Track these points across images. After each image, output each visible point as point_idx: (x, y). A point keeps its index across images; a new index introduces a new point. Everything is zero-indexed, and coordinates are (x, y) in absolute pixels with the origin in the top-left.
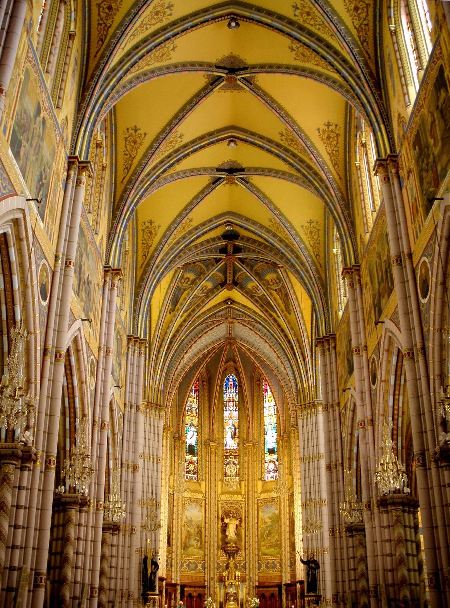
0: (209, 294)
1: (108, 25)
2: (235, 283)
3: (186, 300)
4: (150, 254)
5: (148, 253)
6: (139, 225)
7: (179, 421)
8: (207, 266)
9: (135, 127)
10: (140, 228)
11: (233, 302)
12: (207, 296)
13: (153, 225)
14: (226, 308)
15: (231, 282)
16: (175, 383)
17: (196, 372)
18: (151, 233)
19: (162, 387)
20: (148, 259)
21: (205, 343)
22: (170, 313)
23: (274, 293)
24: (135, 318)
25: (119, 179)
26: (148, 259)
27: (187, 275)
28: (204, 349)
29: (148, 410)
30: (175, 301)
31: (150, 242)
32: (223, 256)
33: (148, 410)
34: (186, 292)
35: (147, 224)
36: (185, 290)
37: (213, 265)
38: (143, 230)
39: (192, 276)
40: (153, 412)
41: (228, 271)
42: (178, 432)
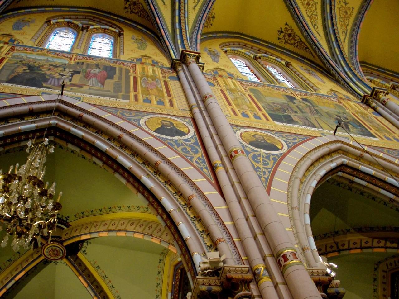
5: (305, 45)
6: (279, 44)
9: (279, 31)
10: (283, 45)
13: (283, 30)
20: (310, 48)
25: (311, 58)
31: (298, 38)
38: (286, 42)
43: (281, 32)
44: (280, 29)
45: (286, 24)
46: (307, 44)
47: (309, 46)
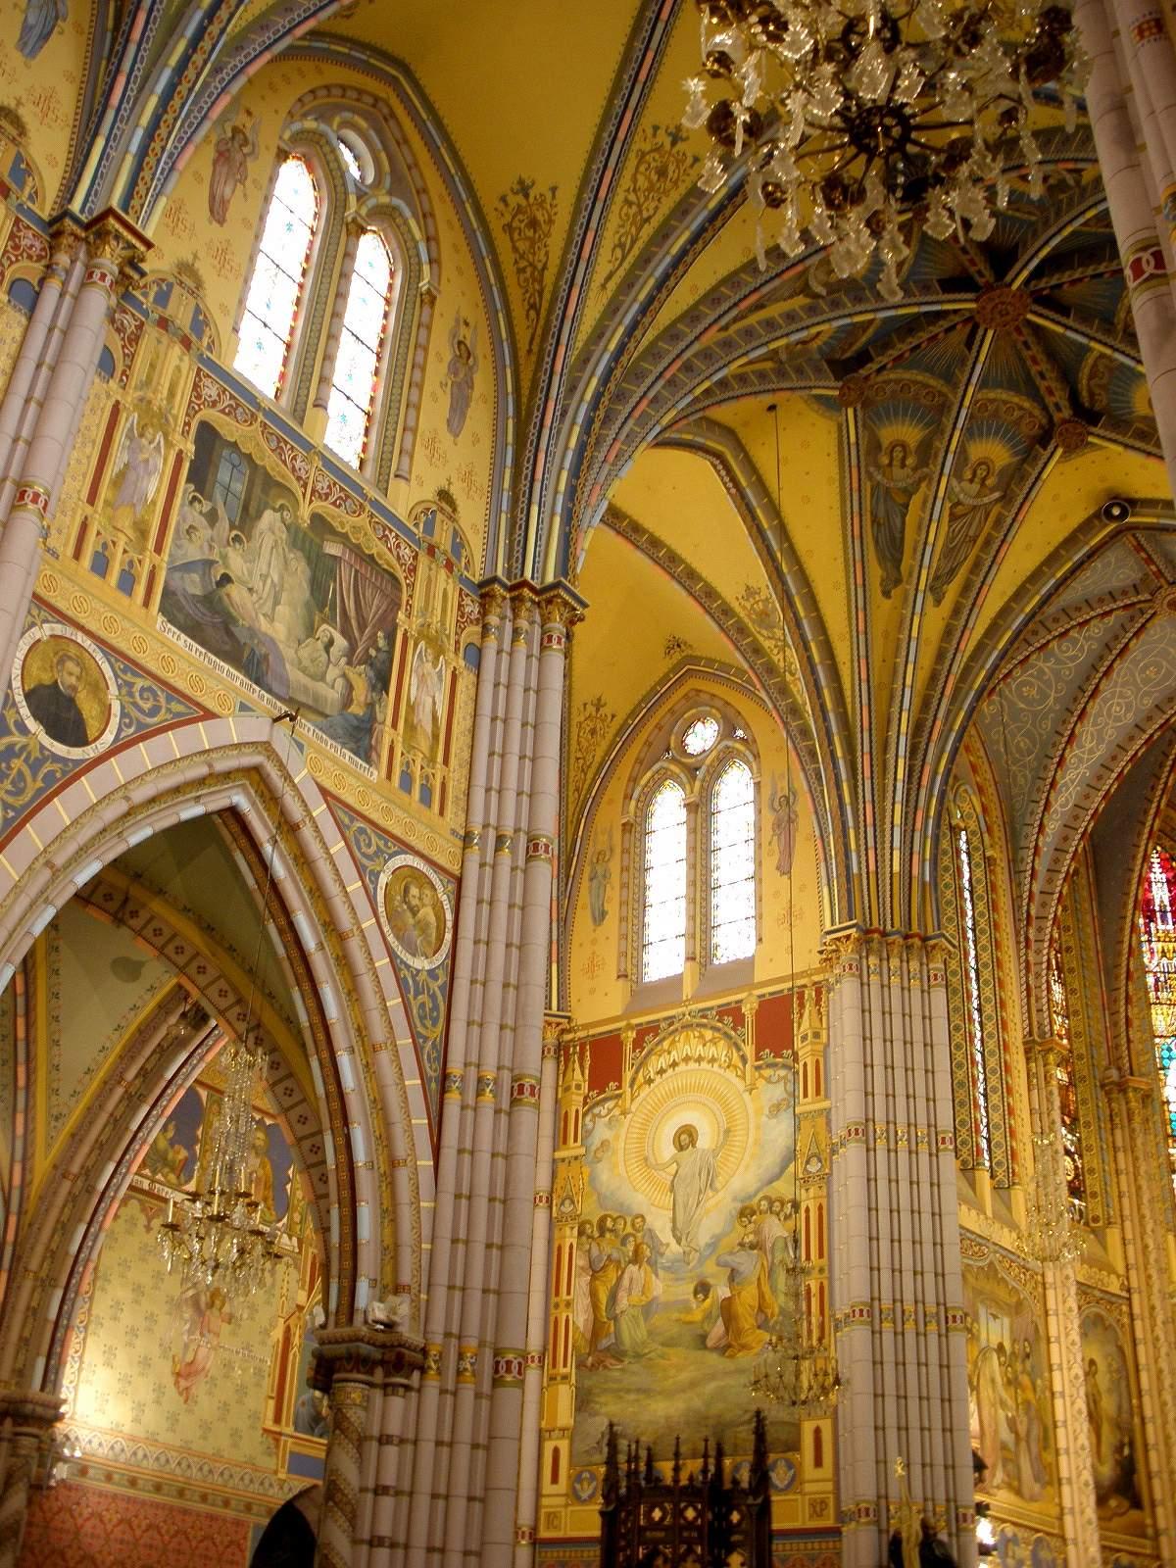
0: (1015, 487)
2: (1087, 415)
3: (929, 532)
4: (547, 296)
5: (541, 293)
7: (1115, 1024)
8: (948, 377)
10: (496, 225)
11: (1129, 504)
12: (1006, 499)
14: (1114, 536)
15: (1067, 413)
16: (1050, 881)
17: (1140, 834)
18: (533, 224)
19: (922, 870)
20: (543, 313)
21: (1130, 718)
22: (887, 594)
24: (518, 527)
26: (543, 313)
27: (889, 434)
28: (1132, 738)
29: (873, 960)
30: (891, 549)
31: (541, 255)
32: (966, 304)
33: (873, 960)
34: (916, 501)
35: (515, 200)
36: (909, 493)
37: (963, 362)
38: (508, 228)
39: (910, 433)
40: (895, 962)
41: (1034, 370)
42: (1115, 1062)
43: (524, 189)
44: (528, 182)
45: (554, 190)
46: (547, 296)
47: (545, 305)
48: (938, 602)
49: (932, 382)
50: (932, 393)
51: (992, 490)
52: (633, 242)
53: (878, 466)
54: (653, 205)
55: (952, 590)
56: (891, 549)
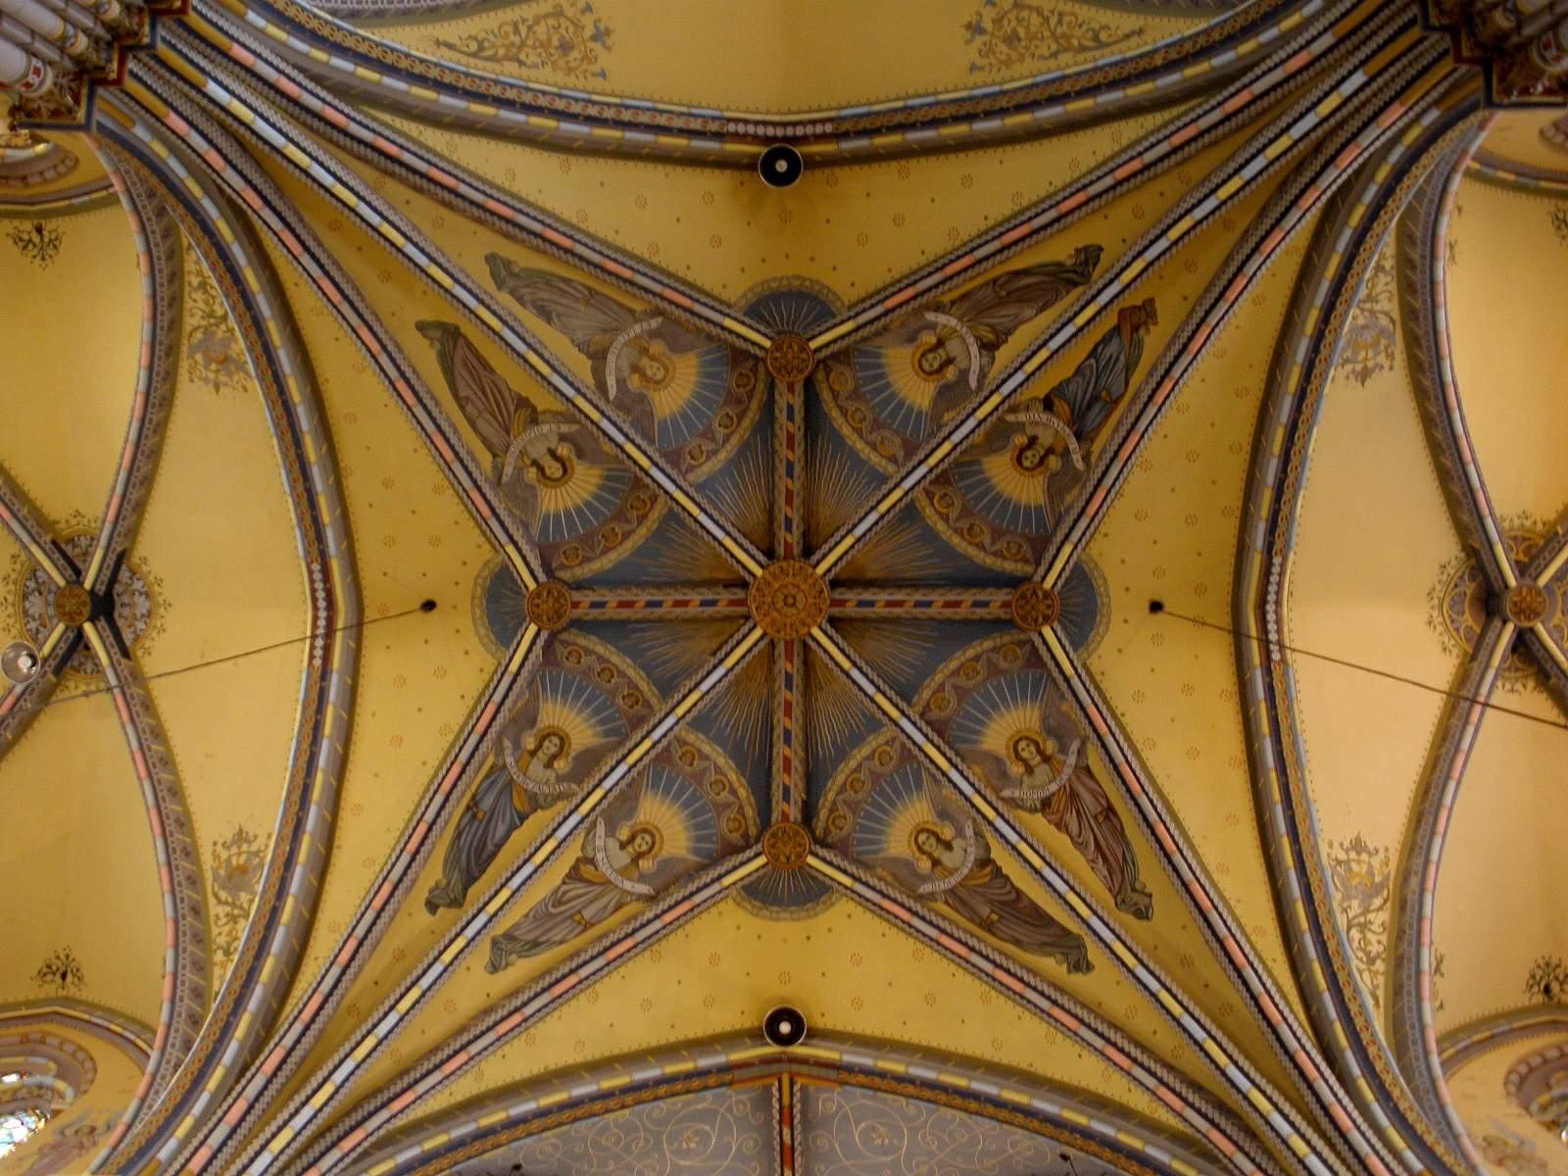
1: (522, 56)
3: (532, 871)
23: (1039, 824)
27: (555, 713)
34: (538, 821)
36: (535, 803)
39: (582, 732)
48: (494, 968)
49: (643, 685)
50: (635, 696)
51: (642, 878)
52: (492, 59)
53: (517, 745)
54: (538, 60)
55: (521, 969)
56: (473, 859)
